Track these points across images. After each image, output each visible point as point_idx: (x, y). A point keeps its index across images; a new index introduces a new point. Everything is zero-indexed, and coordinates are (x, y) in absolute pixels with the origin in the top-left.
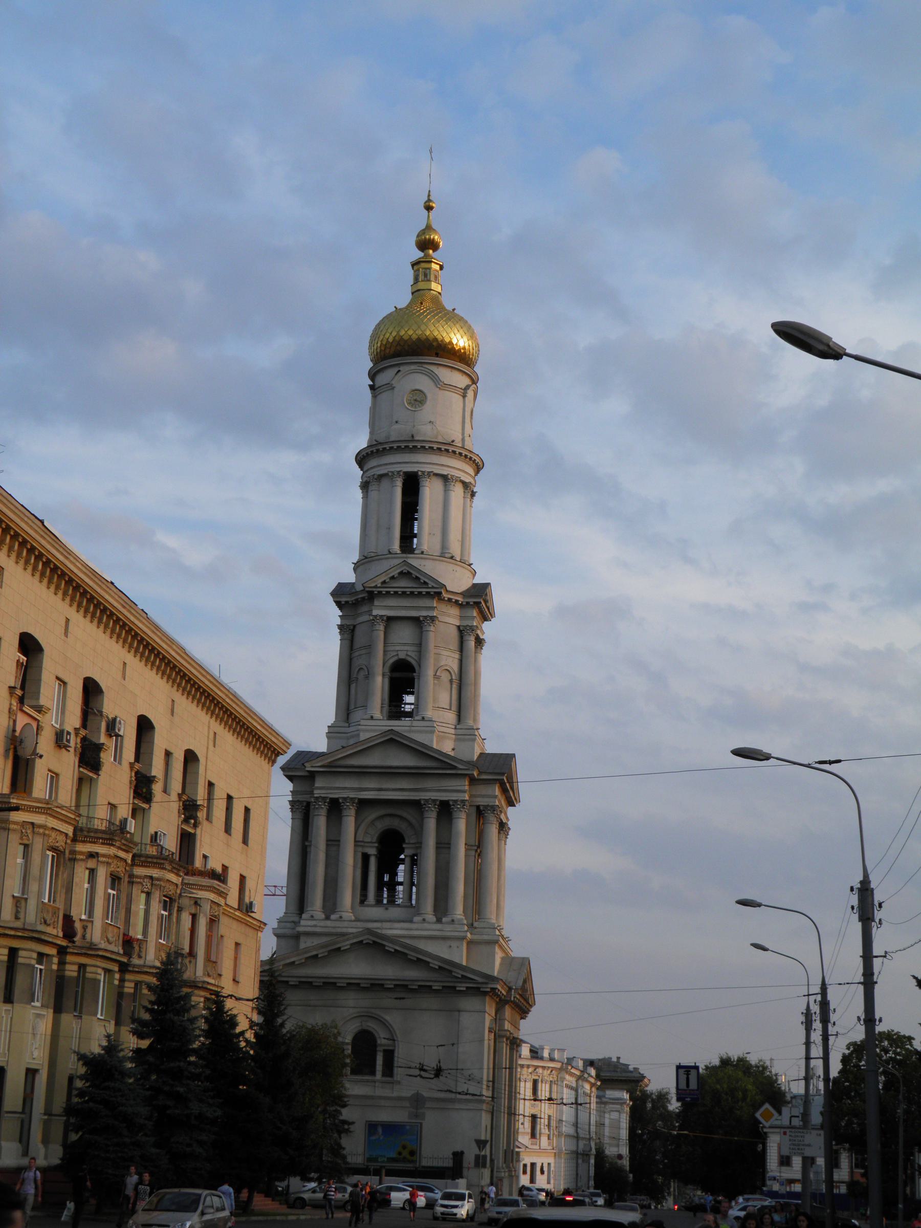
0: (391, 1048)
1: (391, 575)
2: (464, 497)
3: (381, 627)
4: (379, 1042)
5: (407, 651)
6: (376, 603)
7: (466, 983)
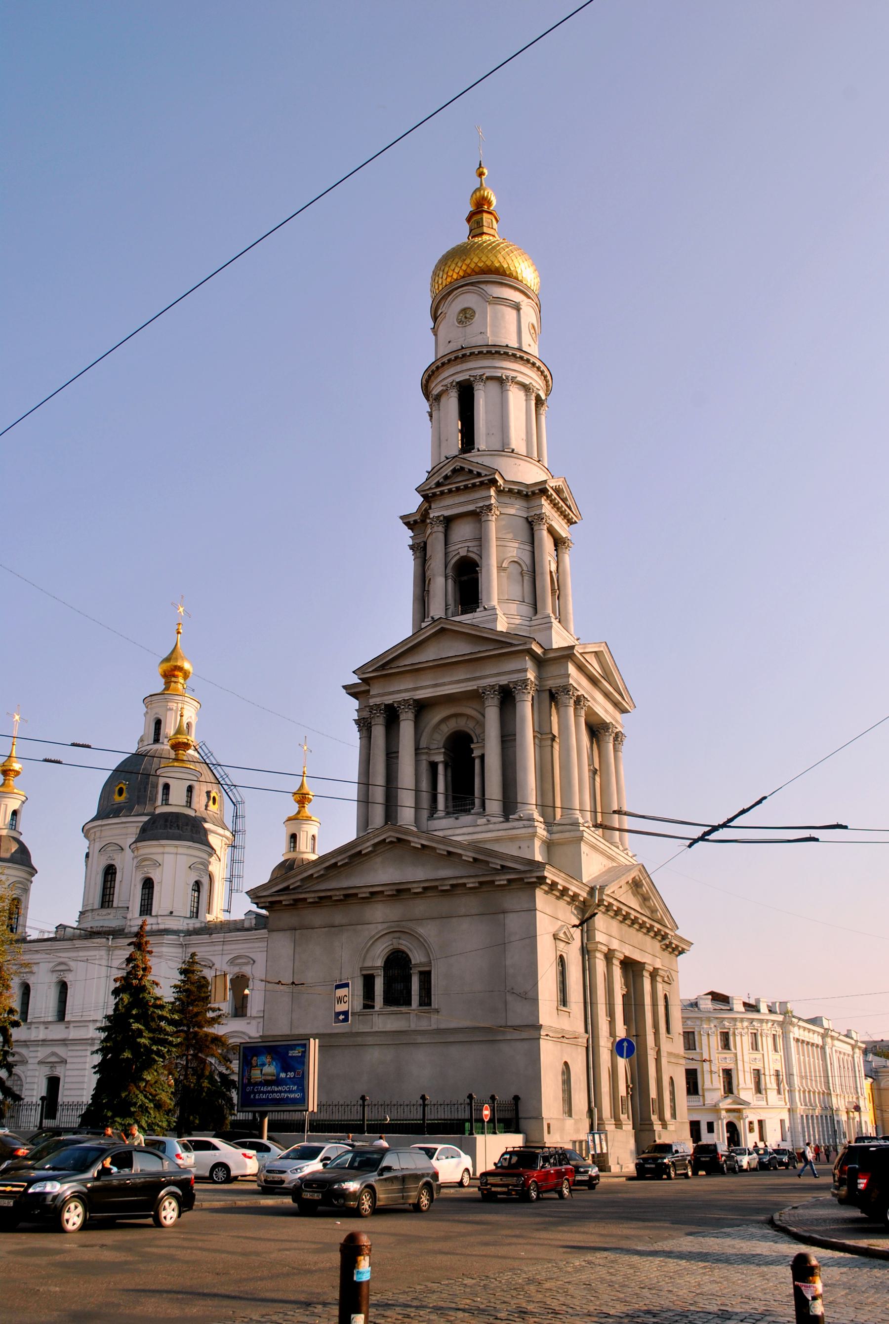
0: (427, 969)
2: (526, 400)
3: (441, 528)
4: (413, 962)
5: (468, 547)
6: (433, 506)
7: (505, 873)
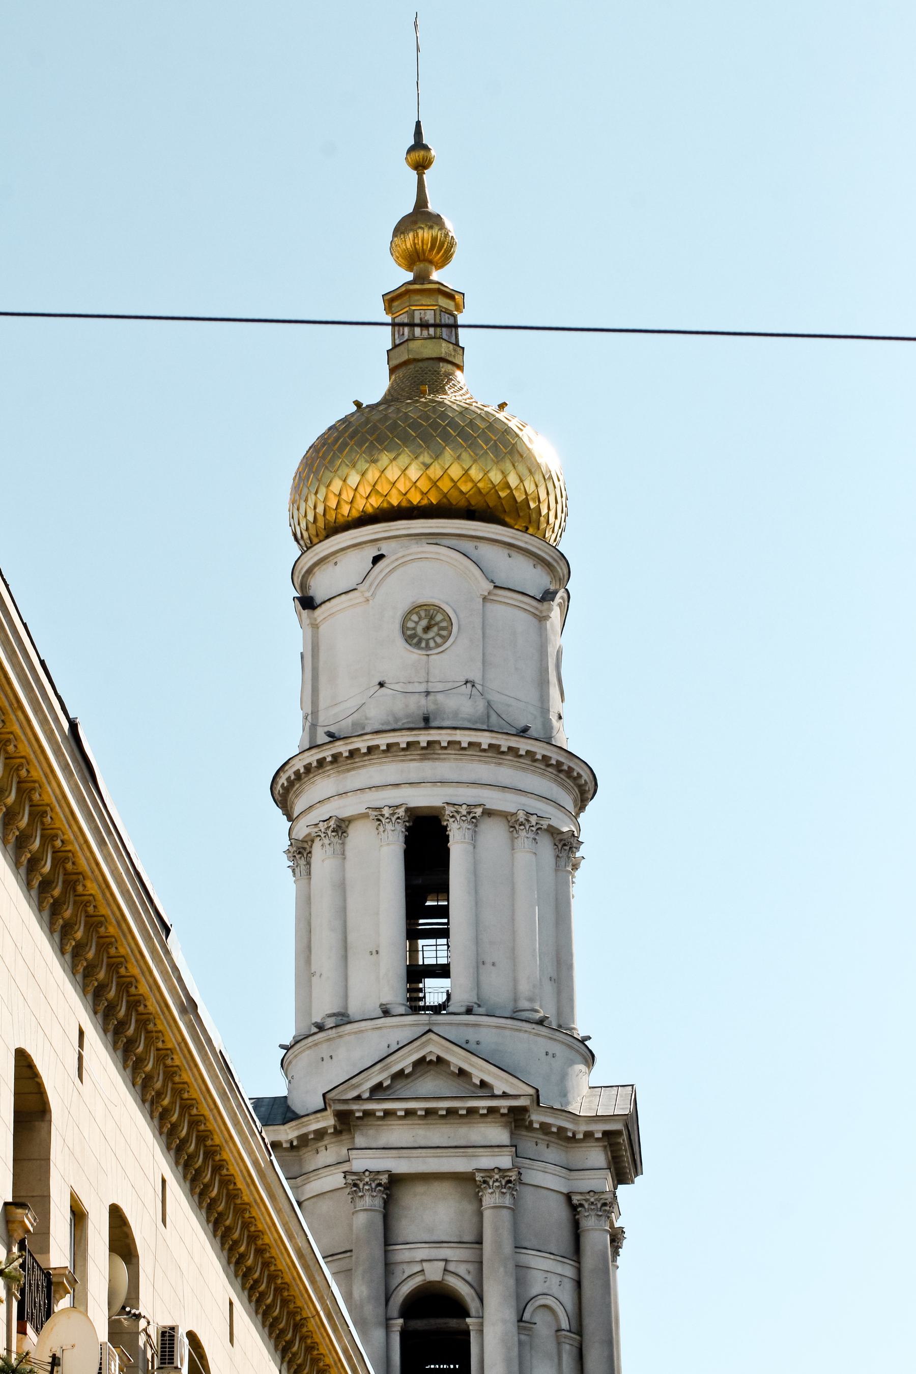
1: (396, 1069)
5: (446, 1261)
